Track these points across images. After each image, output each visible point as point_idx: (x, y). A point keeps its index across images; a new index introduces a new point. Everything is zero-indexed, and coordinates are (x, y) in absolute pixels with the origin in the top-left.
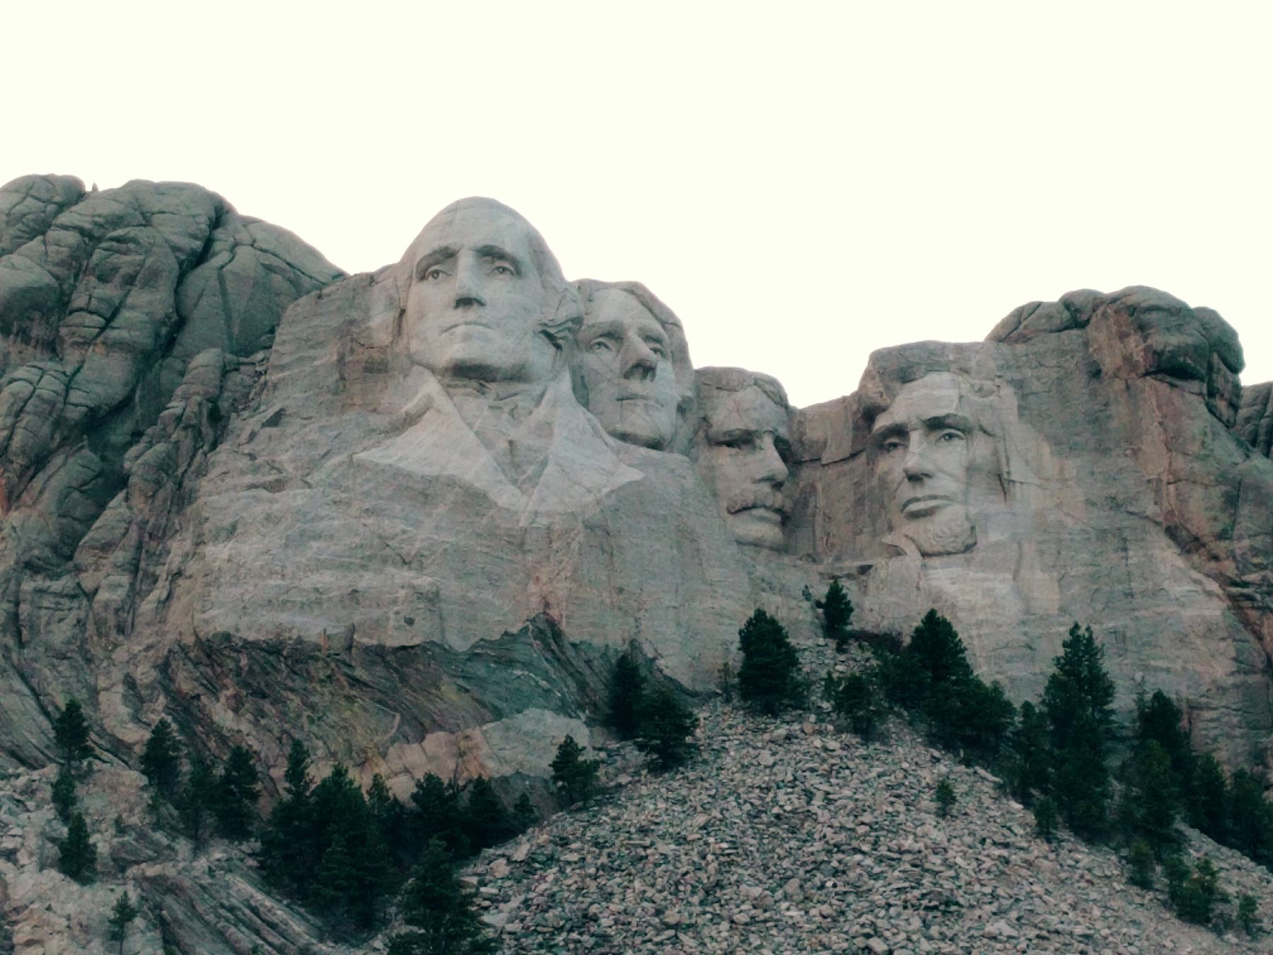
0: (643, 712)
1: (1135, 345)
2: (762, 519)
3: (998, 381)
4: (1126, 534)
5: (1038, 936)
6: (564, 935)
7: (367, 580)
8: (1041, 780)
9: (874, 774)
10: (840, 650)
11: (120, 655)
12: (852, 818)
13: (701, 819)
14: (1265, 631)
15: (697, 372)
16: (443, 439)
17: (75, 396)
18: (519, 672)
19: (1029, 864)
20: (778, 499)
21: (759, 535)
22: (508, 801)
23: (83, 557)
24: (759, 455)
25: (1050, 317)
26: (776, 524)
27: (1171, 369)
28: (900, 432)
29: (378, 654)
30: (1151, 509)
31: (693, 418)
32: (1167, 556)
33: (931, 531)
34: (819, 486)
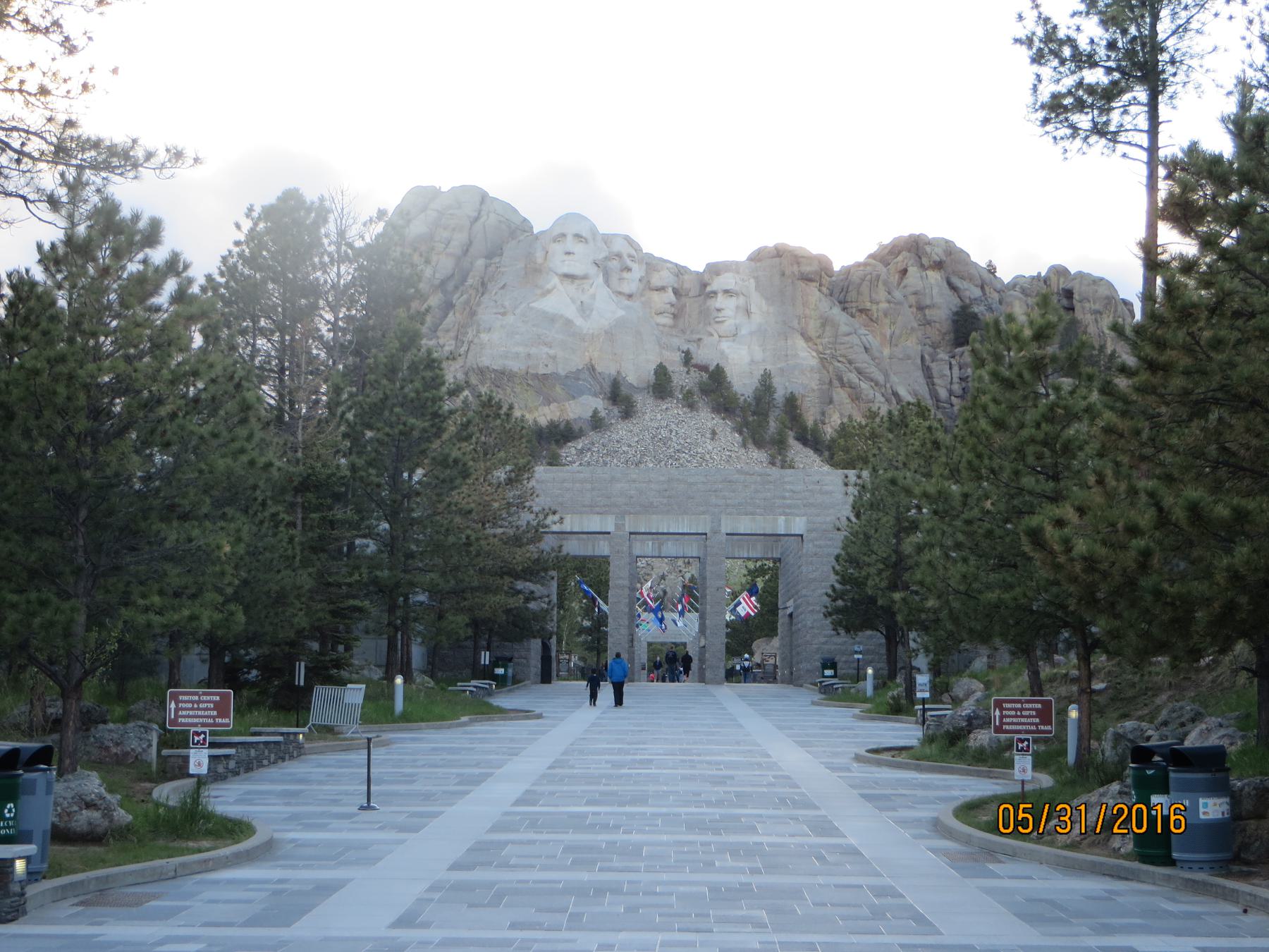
0: (620, 398)
1: (795, 268)
7: (533, 351)
8: (746, 424)
10: (688, 373)
11: (452, 369)
14: (831, 369)
16: (559, 301)
17: (437, 276)
19: (737, 457)
20: (673, 310)
22: (576, 427)
23: (439, 334)
27: (807, 279)
28: (715, 293)
29: (536, 376)
30: (796, 326)
32: (801, 343)
33: (723, 329)
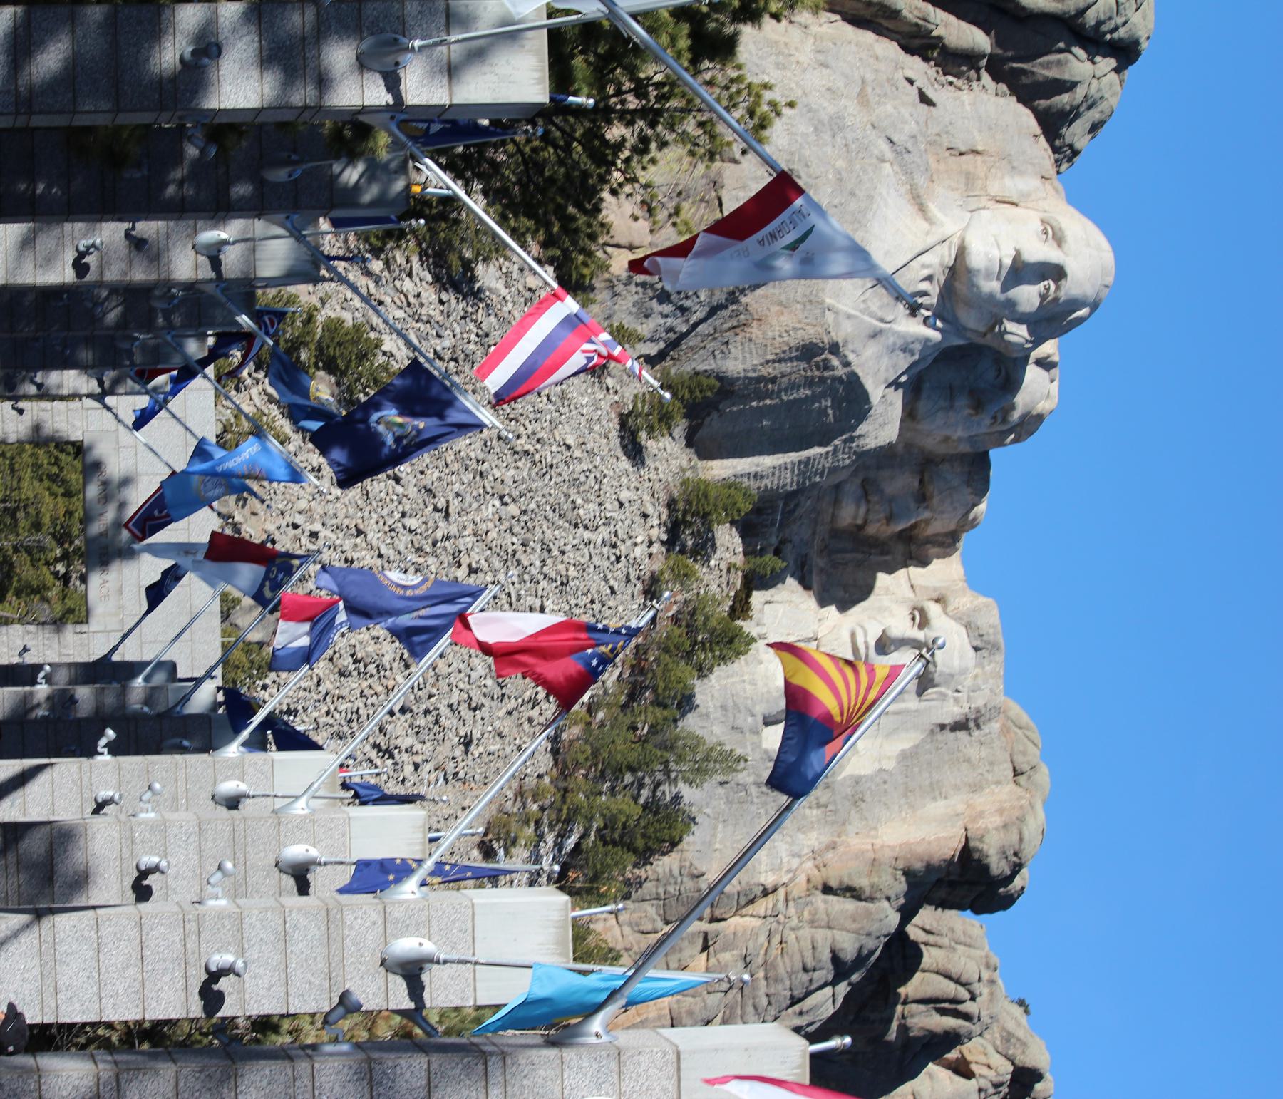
2: (858, 506)
3: (966, 706)
4: (830, 807)
5: (470, 699)
6: (475, 330)
9: (612, 583)
12: (572, 562)
13: (570, 441)
15: (986, 453)
18: (702, 298)
21: (844, 504)
24: (912, 505)
25: (1024, 753)
26: (855, 518)
29: (716, 184)
31: (942, 450)
34: (888, 558)
